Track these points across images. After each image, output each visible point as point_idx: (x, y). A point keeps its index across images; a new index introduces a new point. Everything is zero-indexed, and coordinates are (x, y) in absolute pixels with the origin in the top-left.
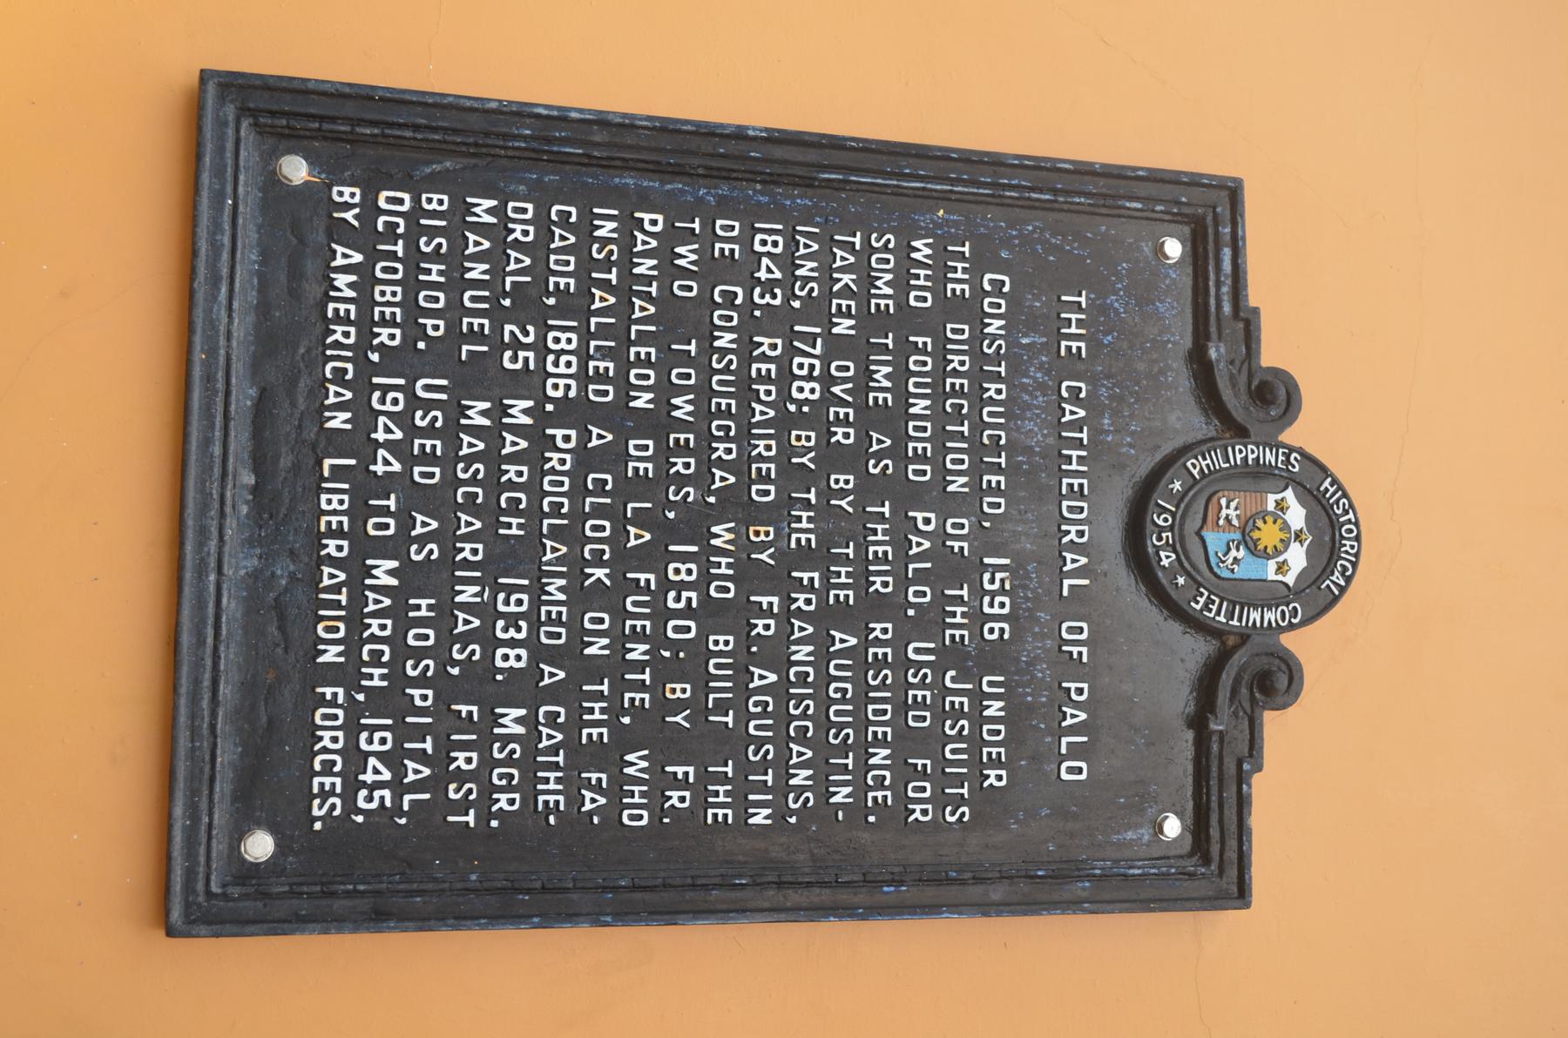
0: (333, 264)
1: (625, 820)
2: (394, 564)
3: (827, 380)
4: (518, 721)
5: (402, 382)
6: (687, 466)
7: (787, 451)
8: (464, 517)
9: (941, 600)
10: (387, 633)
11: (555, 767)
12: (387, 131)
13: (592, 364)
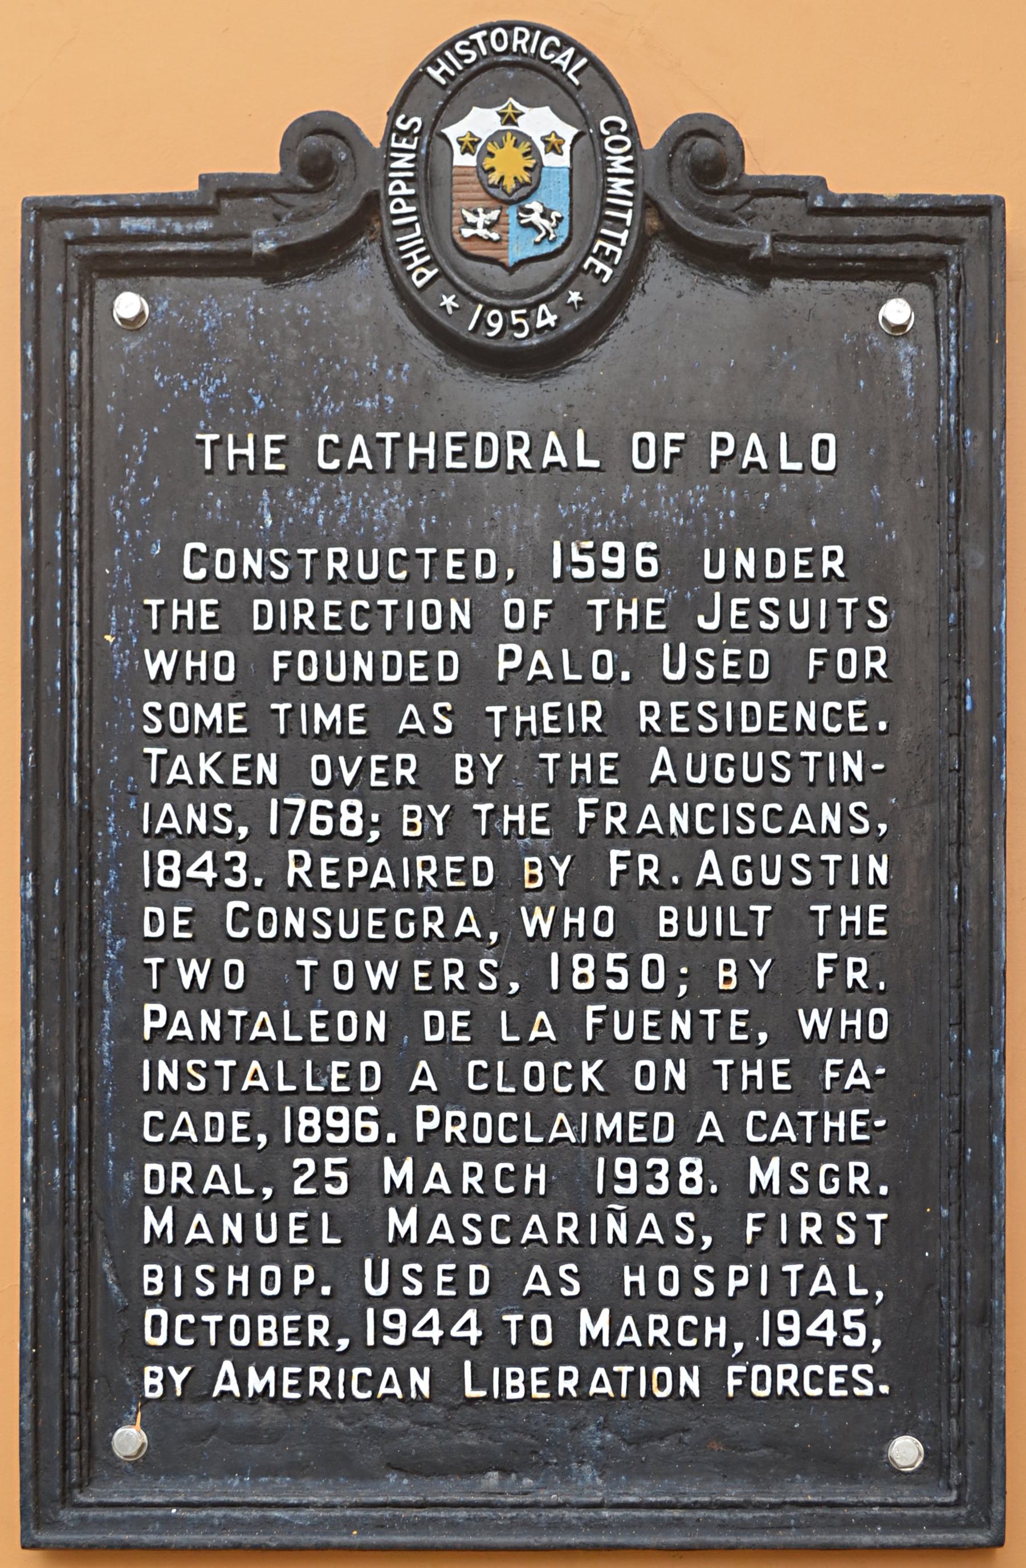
0: (237, 1394)
1: (881, 1035)
2: (585, 1314)
3: (336, 789)
4: (764, 1166)
5: (370, 1312)
6: (453, 968)
7: (428, 842)
8: (527, 1235)
9: (609, 636)
10: (664, 1319)
11: (818, 1120)
12: (73, 1337)
13: (335, 1088)
